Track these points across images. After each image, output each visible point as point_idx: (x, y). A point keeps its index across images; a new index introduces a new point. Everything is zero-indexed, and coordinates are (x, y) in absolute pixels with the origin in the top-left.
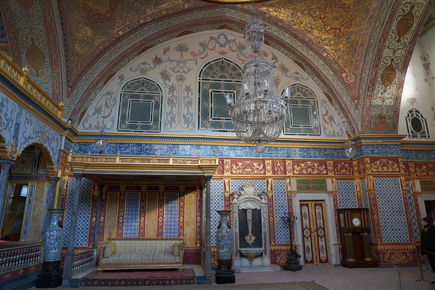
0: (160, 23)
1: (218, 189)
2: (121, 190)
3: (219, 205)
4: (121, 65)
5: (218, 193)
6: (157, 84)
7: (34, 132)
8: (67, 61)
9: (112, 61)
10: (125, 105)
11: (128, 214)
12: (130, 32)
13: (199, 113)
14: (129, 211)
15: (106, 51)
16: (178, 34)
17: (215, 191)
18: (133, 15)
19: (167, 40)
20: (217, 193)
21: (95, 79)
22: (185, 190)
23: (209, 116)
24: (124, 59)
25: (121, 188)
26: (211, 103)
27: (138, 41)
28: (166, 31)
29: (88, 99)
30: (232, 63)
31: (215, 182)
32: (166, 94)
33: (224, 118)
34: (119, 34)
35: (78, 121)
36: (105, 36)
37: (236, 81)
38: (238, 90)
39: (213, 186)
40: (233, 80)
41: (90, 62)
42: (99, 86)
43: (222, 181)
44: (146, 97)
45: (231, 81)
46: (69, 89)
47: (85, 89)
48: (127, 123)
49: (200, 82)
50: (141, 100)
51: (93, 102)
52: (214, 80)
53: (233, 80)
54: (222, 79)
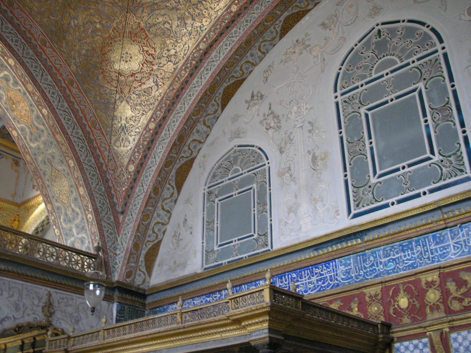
0: (233, 31)
4: (194, 140)
6: (260, 149)
7: (17, 308)
8: (105, 172)
9: (170, 140)
10: (210, 212)
12: (191, 75)
13: (346, 176)
15: (162, 127)
16: (279, 30)
18: (185, 44)
19: (264, 53)
21: (149, 186)
23: (368, 172)
24: (192, 128)
26: (370, 137)
27: (203, 84)
28: (244, 39)
29: (149, 224)
30: (401, 24)
32: (275, 162)
33: (404, 164)
34: (174, 89)
35: (144, 270)
36: (154, 104)
37: (418, 59)
38: (428, 78)
40: (410, 60)
41: (141, 159)
42: (166, 193)
43: (425, 340)
44: (242, 184)
45: (408, 64)
46: (121, 217)
47: (138, 209)
48: (216, 248)
49: (337, 104)
50: (233, 193)
51: (169, 227)
52: (367, 83)
53: (410, 60)
54: (384, 72)
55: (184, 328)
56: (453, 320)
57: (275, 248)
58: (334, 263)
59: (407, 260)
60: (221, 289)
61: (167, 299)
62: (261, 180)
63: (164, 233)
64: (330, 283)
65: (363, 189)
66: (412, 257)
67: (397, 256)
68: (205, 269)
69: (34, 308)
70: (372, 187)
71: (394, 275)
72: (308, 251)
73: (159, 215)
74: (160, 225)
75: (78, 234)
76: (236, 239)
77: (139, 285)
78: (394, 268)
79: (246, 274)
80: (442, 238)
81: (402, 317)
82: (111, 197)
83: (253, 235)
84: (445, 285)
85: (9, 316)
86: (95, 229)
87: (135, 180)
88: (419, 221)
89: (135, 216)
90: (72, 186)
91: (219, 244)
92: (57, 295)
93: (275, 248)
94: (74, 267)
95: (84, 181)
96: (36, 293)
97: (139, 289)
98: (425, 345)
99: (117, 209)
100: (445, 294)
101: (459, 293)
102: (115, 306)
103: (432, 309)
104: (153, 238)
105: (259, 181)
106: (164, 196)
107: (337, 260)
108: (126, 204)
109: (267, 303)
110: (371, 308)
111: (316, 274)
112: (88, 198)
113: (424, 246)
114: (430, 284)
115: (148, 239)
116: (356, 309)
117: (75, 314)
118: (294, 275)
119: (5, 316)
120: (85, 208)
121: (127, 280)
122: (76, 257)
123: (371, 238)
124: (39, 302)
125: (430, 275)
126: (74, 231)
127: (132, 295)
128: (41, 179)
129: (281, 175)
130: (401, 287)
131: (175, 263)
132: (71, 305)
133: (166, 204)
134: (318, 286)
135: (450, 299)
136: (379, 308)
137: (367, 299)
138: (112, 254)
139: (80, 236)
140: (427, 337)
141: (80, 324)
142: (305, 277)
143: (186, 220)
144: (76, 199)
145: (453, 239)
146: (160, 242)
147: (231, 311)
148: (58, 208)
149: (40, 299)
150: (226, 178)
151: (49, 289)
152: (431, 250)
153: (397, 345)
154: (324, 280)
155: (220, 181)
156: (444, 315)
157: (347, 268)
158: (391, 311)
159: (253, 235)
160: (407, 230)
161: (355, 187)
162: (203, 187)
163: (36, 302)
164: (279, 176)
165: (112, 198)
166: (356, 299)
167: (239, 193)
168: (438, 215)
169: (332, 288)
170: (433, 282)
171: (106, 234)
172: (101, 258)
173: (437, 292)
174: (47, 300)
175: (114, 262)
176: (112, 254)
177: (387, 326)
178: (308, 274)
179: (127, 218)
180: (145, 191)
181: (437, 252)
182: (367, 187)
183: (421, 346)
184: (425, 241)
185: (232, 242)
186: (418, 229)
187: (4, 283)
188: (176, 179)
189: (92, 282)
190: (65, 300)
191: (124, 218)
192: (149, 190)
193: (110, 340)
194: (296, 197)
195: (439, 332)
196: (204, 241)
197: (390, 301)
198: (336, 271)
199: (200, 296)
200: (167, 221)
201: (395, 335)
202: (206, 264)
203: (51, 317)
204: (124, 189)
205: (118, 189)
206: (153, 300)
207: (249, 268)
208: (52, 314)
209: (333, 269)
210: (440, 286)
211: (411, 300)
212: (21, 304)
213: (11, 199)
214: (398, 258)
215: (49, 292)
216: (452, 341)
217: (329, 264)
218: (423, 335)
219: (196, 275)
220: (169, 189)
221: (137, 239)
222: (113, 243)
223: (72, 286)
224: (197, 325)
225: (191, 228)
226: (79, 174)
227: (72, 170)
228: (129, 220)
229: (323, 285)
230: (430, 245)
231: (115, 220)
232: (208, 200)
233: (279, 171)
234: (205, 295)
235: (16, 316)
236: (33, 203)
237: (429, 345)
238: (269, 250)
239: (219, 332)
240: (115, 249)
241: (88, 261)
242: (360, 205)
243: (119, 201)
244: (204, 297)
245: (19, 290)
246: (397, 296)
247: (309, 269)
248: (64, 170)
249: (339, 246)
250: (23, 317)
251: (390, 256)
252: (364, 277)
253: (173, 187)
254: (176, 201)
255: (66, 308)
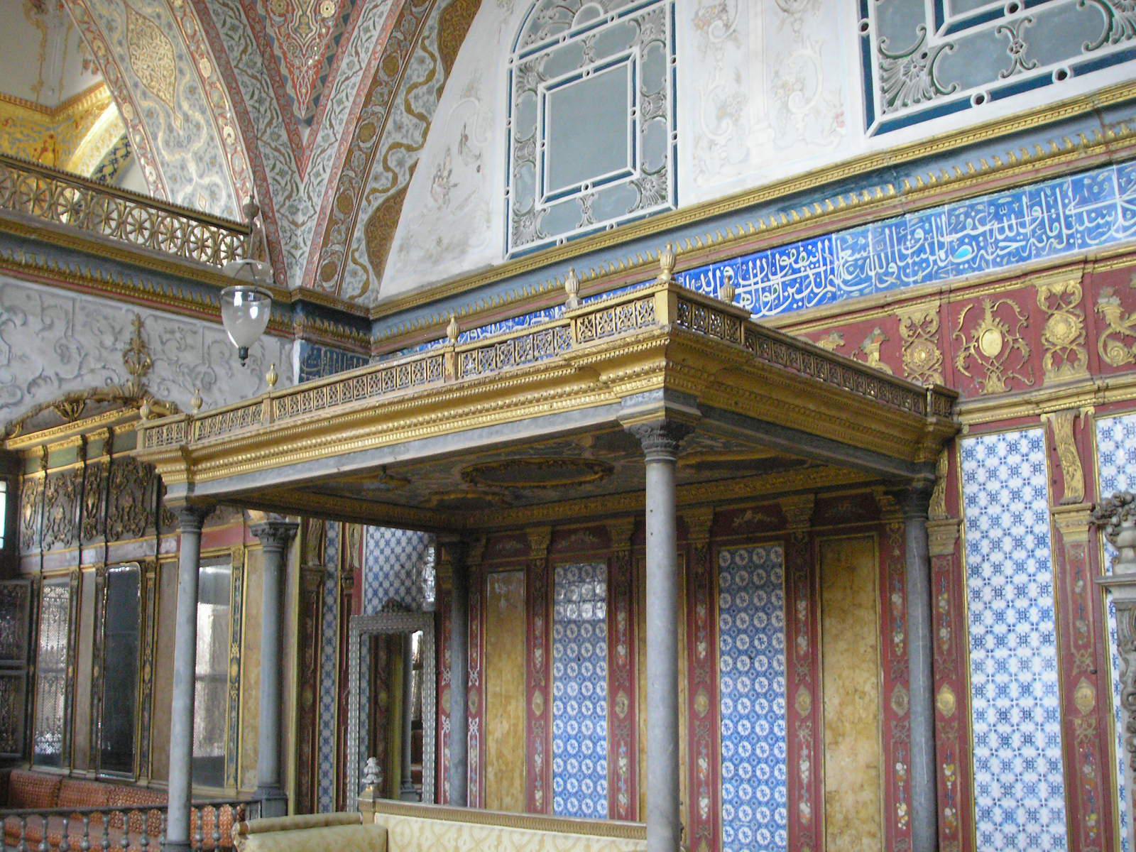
1: (1016, 495)
2: (533, 555)
3: (1022, 603)
5: (1018, 519)
7: (64, 356)
8: (261, 20)
10: (526, 118)
11: (565, 678)
14: (566, 661)
17: (994, 510)
20: (1006, 520)
21: (374, 52)
22: (813, 521)
25: (533, 539)
29: (376, 146)
31: (991, 450)
35: (365, 260)
39: (981, 475)
42: (416, 72)
43: (1036, 433)
46: (306, 133)
47: (347, 111)
48: (539, 206)
50: (583, 70)
51: (424, 156)
55: (461, 388)
56: (1107, 388)
57: (683, 204)
58: (827, 243)
59: (1006, 240)
60: (552, 303)
61: (422, 328)
62: (653, 37)
63: (412, 169)
64: (816, 290)
65: (906, 60)
66: (1018, 234)
67: (981, 229)
68: (513, 256)
69: (105, 353)
70: (930, 57)
71: (972, 277)
72: (764, 212)
73: (399, 127)
74: (403, 149)
75: (201, 176)
76: (588, 182)
77: (352, 298)
78: (974, 259)
79: (612, 268)
80: (1096, 189)
81: (984, 376)
82: (279, 82)
83: (629, 174)
84: (1095, 303)
85: (45, 373)
86: (242, 162)
87: (337, 39)
88: (1040, 146)
89: (340, 129)
90: (180, 57)
91: (546, 194)
92: (157, 323)
93: (683, 204)
94: (195, 254)
95: (212, 44)
96: (106, 318)
97: (352, 306)
98: (1035, 445)
99: (296, 113)
100: (1093, 324)
101: (1127, 324)
102: (297, 346)
103: (1057, 361)
104: (384, 182)
105: (647, 39)
106: (410, 78)
107: (834, 236)
108: (316, 100)
109: (663, 327)
110: (912, 355)
111: (782, 268)
112: (221, 86)
113: (1049, 208)
114: (1057, 301)
115: (372, 184)
116: (876, 355)
117: (203, 369)
118: (729, 271)
119: (37, 374)
120: (217, 111)
121: (325, 284)
122: (197, 231)
123: (921, 184)
124: (116, 340)
125: (1060, 278)
126: (192, 168)
127: (337, 322)
128: (103, 40)
129: (701, 23)
130: (987, 305)
131: (439, 241)
132: (192, 348)
133: (416, 98)
134: (786, 299)
135: (1104, 336)
136: (930, 354)
137: (904, 331)
138: (285, 223)
139: (206, 181)
140: (1040, 425)
141: (215, 389)
142: (755, 275)
143: (465, 138)
144: (192, 90)
145: (1122, 190)
146: (403, 191)
147: (575, 346)
148: (150, 114)
149: (117, 335)
150: (566, 33)
151: (137, 309)
152: (1066, 217)
153: (968, 443)
154: (800, 284)
155: (549, 40)
156: (1088, 376)
157: (857, 256)
158: (960, 363)
159: (629, 174)
160: (1012, 166)
161: (887, 57)
162: (508, 56)
163: (108, 340)
164: (697, 27)
165: (283, 86)
166: (877, 331)
167: (596, 70)
168: (1090, 132)
169: (819, 302)
170: (1065, 296)
171: (269, 175)
172: (260, 232)
173: (1072, 319)
174: (135, 337)
175: (292, 244)
176: (285, 223)
177: (947, 398)
178: (762, 269)
179: (321, 134)
180: (364, 66)
181: (1082, 223)
182: (917, 56)
183: (1024, 446)
184: (1054, 194)
185: (578, 190)
186: (1038, 165)
187: (29, 297)
188: (440, 35)
189: (239, 287)
190: (178, 335)
191: (314, 134)
192: (374, 64)
193: (288, 421)
194: (738, 79)
195: (1070, 416)
196: (511, 189)
197: (958, 339)
198: (832, 262)
199: (500, 322)
200: (420, 140)
201: (965, 420)
202: (515, 244)
203: (145, 374)
204: (311, 62)
205: (297, 62)
206: (388, 333)
207: (620, 253)
208: (147, 368)
209: (824, 259)
210: (1082, 305)
211: (1010, 338)
212: (73, 347)
213: (31, 97)
214: (984, 234)
215: (138, 317)
216: (1099, 436)
217: (815, 245)
218: (1033, 421)
219: (491, 270)
220: (422, 61)
221: (347, 185)
222: (289, 197)
223: (192, 302)
224: (492, 381)
225: (479, 157)
226: (198, 26)
227: (179, 15)
228: (325, 138)
229: (797, 297)
230: (1065, 206)
231: (291, 141)
232: (521, 86)
233: (697, 14)
234: (514, 318)
235: (63, 375)
236: (85, 104)
237: (1043, 444)
238: (669, 209)
239: (546, 399)
240: (294, 210)
241: (228, 240)
242: (898, 103)
243: (300, 93)
244: (510, 323)
245: (67, 313)
246: (976, 325)
247: (767, 257)
248: (159, 16)
249: (841, 202)
250: (79, 375)
251: (964, 228)
252: (898, 278)
253: (432, 56)
254: (440, 91)
255: (181, 355)
